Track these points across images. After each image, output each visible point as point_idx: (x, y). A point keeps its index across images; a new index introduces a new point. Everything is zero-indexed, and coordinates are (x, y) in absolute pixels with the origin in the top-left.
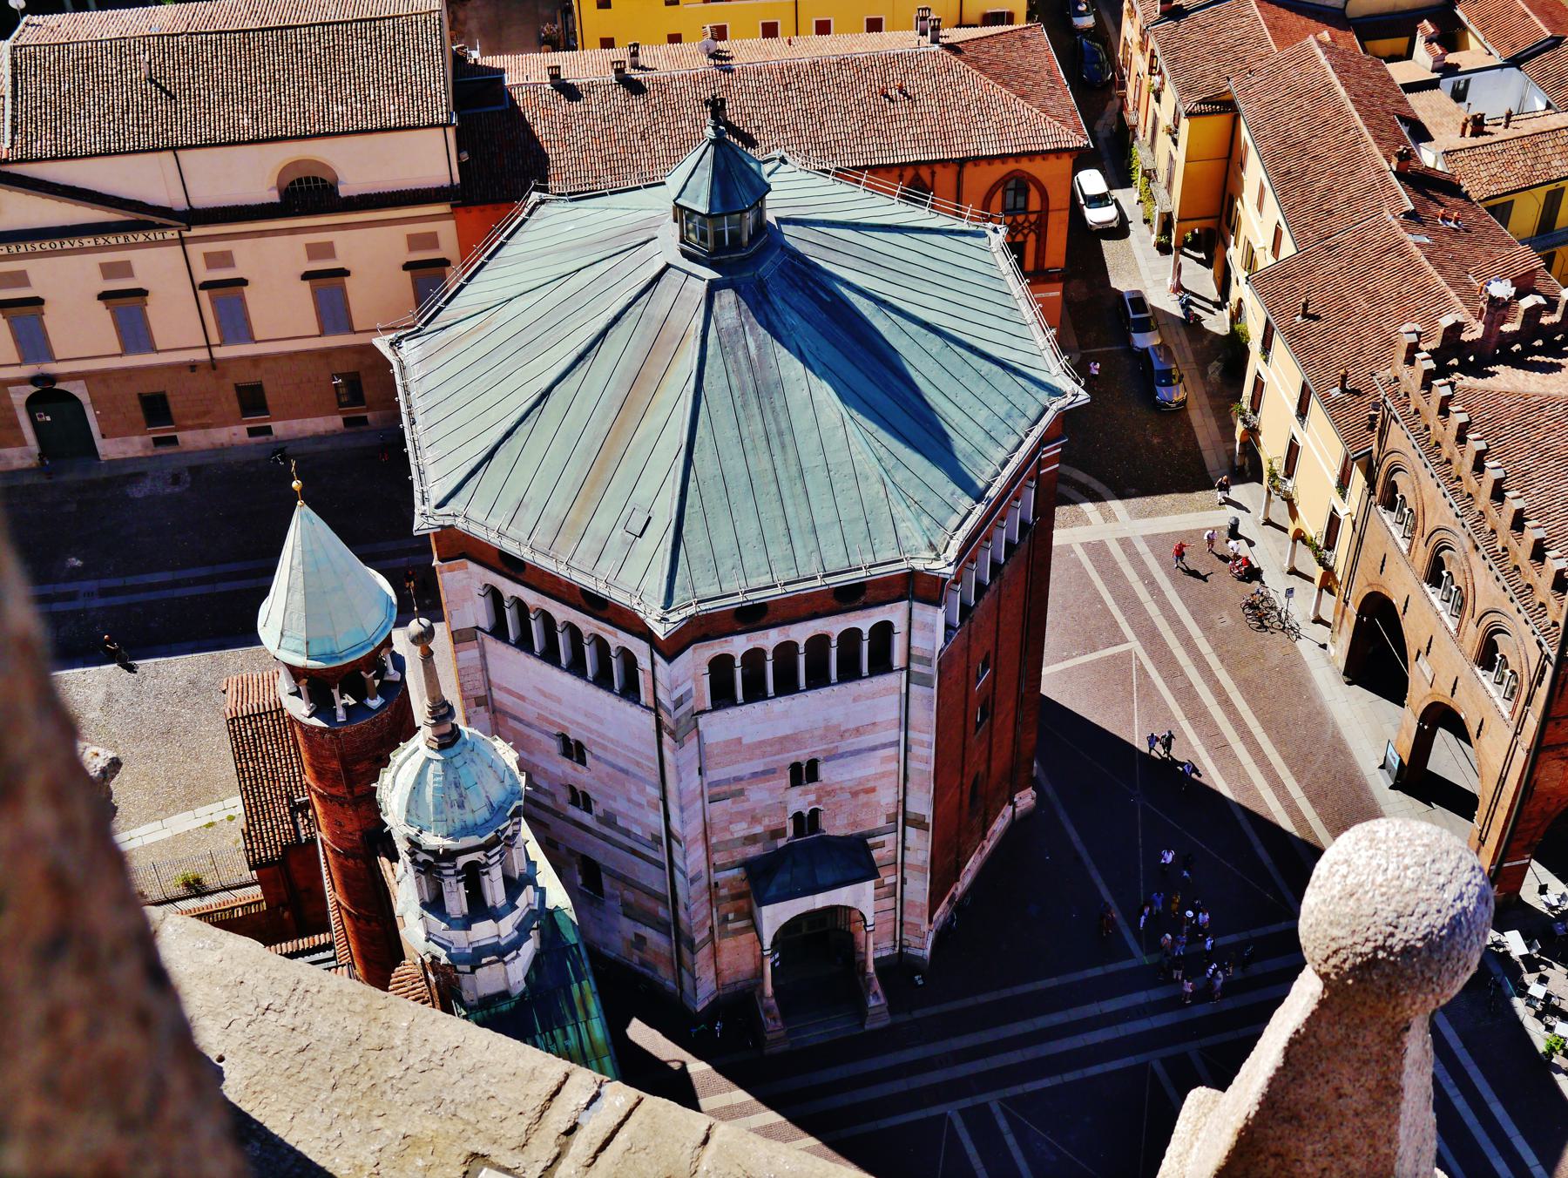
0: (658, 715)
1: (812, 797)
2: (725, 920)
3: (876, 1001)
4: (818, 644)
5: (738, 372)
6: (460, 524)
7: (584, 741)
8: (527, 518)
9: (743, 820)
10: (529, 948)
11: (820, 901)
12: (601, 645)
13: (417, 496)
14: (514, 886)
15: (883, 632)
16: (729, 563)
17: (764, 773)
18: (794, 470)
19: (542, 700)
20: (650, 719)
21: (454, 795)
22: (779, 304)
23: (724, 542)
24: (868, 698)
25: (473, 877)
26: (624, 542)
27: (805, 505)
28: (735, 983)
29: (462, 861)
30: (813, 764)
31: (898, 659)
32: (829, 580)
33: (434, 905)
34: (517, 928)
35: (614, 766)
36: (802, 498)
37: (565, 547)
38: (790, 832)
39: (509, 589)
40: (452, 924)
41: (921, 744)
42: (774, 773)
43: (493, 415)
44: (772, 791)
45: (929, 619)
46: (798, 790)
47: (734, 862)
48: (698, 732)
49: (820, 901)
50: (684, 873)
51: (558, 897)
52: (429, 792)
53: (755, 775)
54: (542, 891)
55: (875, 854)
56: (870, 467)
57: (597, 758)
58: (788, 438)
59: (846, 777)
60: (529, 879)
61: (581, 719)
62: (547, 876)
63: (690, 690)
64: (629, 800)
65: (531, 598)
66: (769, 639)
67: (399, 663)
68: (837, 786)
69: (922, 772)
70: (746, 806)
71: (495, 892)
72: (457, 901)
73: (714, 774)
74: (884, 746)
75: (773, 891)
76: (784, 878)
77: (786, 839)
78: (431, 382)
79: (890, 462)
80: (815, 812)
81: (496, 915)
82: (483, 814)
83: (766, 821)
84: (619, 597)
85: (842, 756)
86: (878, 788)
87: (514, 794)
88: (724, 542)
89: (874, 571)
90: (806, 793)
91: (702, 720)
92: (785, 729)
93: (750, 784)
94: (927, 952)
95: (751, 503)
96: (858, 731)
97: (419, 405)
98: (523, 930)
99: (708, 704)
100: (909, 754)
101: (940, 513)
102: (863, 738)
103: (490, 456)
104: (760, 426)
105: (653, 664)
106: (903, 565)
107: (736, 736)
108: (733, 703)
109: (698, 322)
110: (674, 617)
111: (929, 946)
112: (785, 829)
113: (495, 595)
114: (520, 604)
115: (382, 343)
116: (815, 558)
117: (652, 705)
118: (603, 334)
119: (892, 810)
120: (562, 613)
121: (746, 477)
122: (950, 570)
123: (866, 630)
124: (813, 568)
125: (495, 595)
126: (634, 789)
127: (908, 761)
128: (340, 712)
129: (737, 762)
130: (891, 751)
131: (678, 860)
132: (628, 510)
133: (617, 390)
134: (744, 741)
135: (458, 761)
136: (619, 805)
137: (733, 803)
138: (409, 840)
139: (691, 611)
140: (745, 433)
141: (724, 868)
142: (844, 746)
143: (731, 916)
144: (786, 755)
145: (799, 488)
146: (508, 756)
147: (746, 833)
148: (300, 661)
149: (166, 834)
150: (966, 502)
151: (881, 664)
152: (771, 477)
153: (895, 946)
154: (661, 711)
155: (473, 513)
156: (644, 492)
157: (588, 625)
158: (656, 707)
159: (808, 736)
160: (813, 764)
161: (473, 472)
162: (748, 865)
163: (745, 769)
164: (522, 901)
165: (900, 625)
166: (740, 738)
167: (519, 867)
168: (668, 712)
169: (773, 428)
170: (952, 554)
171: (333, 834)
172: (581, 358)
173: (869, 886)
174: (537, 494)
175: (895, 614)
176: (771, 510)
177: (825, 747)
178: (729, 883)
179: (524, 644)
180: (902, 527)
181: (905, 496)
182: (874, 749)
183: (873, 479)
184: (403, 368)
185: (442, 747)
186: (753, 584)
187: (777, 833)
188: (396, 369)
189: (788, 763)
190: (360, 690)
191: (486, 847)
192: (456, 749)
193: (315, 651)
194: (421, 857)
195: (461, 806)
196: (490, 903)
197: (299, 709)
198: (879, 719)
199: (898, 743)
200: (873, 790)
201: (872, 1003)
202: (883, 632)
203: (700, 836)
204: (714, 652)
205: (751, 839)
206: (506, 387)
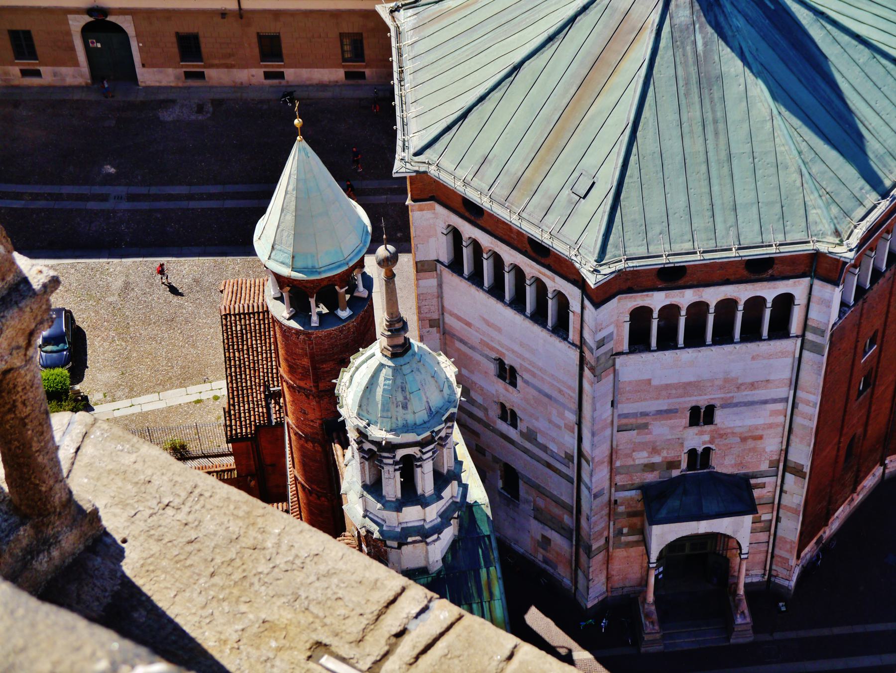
0: (582, 352)
1: (707, 438)
2: (620, 533)
3: (743, 619)
4: (727, 307)
5: (685, 64)
6: (433, 171)
7: (517, 367)
8: (490, 172)
9: (643, 450)
10: (449, 534)
11: (703, 527)
12: (541, 288)
13: (399, 143)
14: (442, 480)
15: (785, 302)
16: (657, 229)
17: (668, 412)
18: (723, 155)
19: (484, 327)
20: (574, 355)
21: (400, 398)
22: (729, 8)
23: (655, 210)
24: (764, 358)
25: (408, 467)
26: (570, 201)
27: (729, 186)
28: (623, 588)
29: (400, 453)
30: (710, 409)
31: (795, 327)
32: (743, 253)
33: (374, 488)
34: (441, 516)
35: (540, 391)
36: (728, 180)
37: (519, 199)
38: (684, 465)
39: (469, 231)
40: (386, 505)
41: (807, 403)
42: (677, 412)
43: (471, 81)
44: (672, 428)
45: (827, 296)
46: (695, 429)
47: (632, 484)
48: (615, 370)
49: (703, 527)
50: (589, 489)
51: (478, 493)
52: (379, 391)
53: (659, 412)
54: (465, 487)
55: (756, 493)
56: (790, 156)
57: (526, 382)
58: (721, 126)
59: (738, 423)
60: (455, 475)
61: (516, 348)
62: (471, 475)
63: (612, 334)
64: (550, 421)
65: (486, 241)
66: (685, 298)
67: (368, 282)
68: (729, 431)
69: (804, 427)
70: (648, 438)
71: (425, 482)
72: (392, 486)
73: (624, 408)
74: (775, 401)
75: (663, 513)
76: (674, 503)
77: (680, 470)
78: (421, 47)
79: (809, 156)
80: (707, 451)
81: (424, 502)
82: (422, 416)
83: (664, 453)
84: (559, 247)
85: (736, 405)
86: (765, 437)
87: (450, 402)
88: (655, 210)
89: (783, 249)
90: (701, 433)
91: (619, 360)
92: (689, 377)
93: (656, 419)
94: (793, 584)
95: (682, 179)
96: (753, 386)
97: (408, 66)
98: (445, 518)
99: (625, 347)
100: (796, 410)
101: (848, 204)
102: (757, 392)
103: (464, 116)
104: (698, 114)
105: (583, 308)
106: (810, 247)
107: (646, 377)
108: (647, 348)
109: (655, 17)
110: (605, 270)
111: (795, 578)
112: (680, 462)
113: (456, 235)
114: (476, 246)
115: (383, 10)
116: (733, 232)
117: (578, 343)
118: (572, 20)
119: (775, 457)
120: (510, 256)
121: (681, 156)
122: (851, 255)
124: (731, 241)
125: (456, 235)
126: (554, 412)
127: (794, 417)
128: (315, 320)
129: (645, 400)
131: (585, 477)
132: (576, 174)
133: (579, 69)
134: (655, 382)
135: (406, 369)
136: (540, 425)
137: (638, 434)
138: (359, 431)
139: (620, 266)
140: (684, 118)
141: (624, 488)
142: (741, 396)
143: (625, 530)
144: (688, 399)
145: (726, 170)
146: (449, 370)
147: (646, 461)
148: (286, 271)
149: (161, 405)
150: (872, 197)
151: (780, 330)
152: (702, 158)
153: (764, 574)
154: (585, 349)
155: (446, 163)
156: (591, 161)
157: (531, 268)
158: (581, 346)
159: (709, 384)
160: (710, 409)
161: (448, 128)
162: (645, 489)
163: (652, 406)
164: (447, 493)
165: (800, 298)
166: (649, 381)
167: (447, 464)
168: (591, 350)
169: (709, 116)
170: (854, 241)
171: (297, 419)
172: (550, 39)
173: (748, 519)
174: (500, 153)
175: (797, 288)
176: (699, 187)
177: (722, 396)
178: (627, 502)
179: (476, 278)
180: (813, 214)
181: (819, 186)
182: (765, 402)
183: (793, 169)
184: (399, 33)
185: (394, 356)
186: (677, 248)
187: (672, 464)
188: (393, 33)
189: (690, 405)
190: (333, 303)
191: (422, 444)
192: (406, 358)
193: (299, 264)
194: (367, 446)
195: (405, 407)
196: (420, 491)
197: (281, 311)
198: (772, 377)
199: (786, 400)
200: (760, 437)
201: (739, 620)
202: (785, 302)
203: (607, 459)
204: (635, 303)
206: (483, 58)
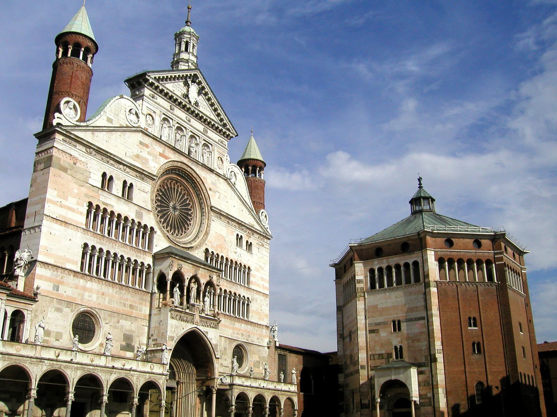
1: (399, 339)
80: (401, 347)
90: (397, 337)
100: (429, 323)
119: (426, 354)
123: (411, 263)
130: (421, 322)
134: (379, 307)
187: (389, 355)
205: (381, 356)
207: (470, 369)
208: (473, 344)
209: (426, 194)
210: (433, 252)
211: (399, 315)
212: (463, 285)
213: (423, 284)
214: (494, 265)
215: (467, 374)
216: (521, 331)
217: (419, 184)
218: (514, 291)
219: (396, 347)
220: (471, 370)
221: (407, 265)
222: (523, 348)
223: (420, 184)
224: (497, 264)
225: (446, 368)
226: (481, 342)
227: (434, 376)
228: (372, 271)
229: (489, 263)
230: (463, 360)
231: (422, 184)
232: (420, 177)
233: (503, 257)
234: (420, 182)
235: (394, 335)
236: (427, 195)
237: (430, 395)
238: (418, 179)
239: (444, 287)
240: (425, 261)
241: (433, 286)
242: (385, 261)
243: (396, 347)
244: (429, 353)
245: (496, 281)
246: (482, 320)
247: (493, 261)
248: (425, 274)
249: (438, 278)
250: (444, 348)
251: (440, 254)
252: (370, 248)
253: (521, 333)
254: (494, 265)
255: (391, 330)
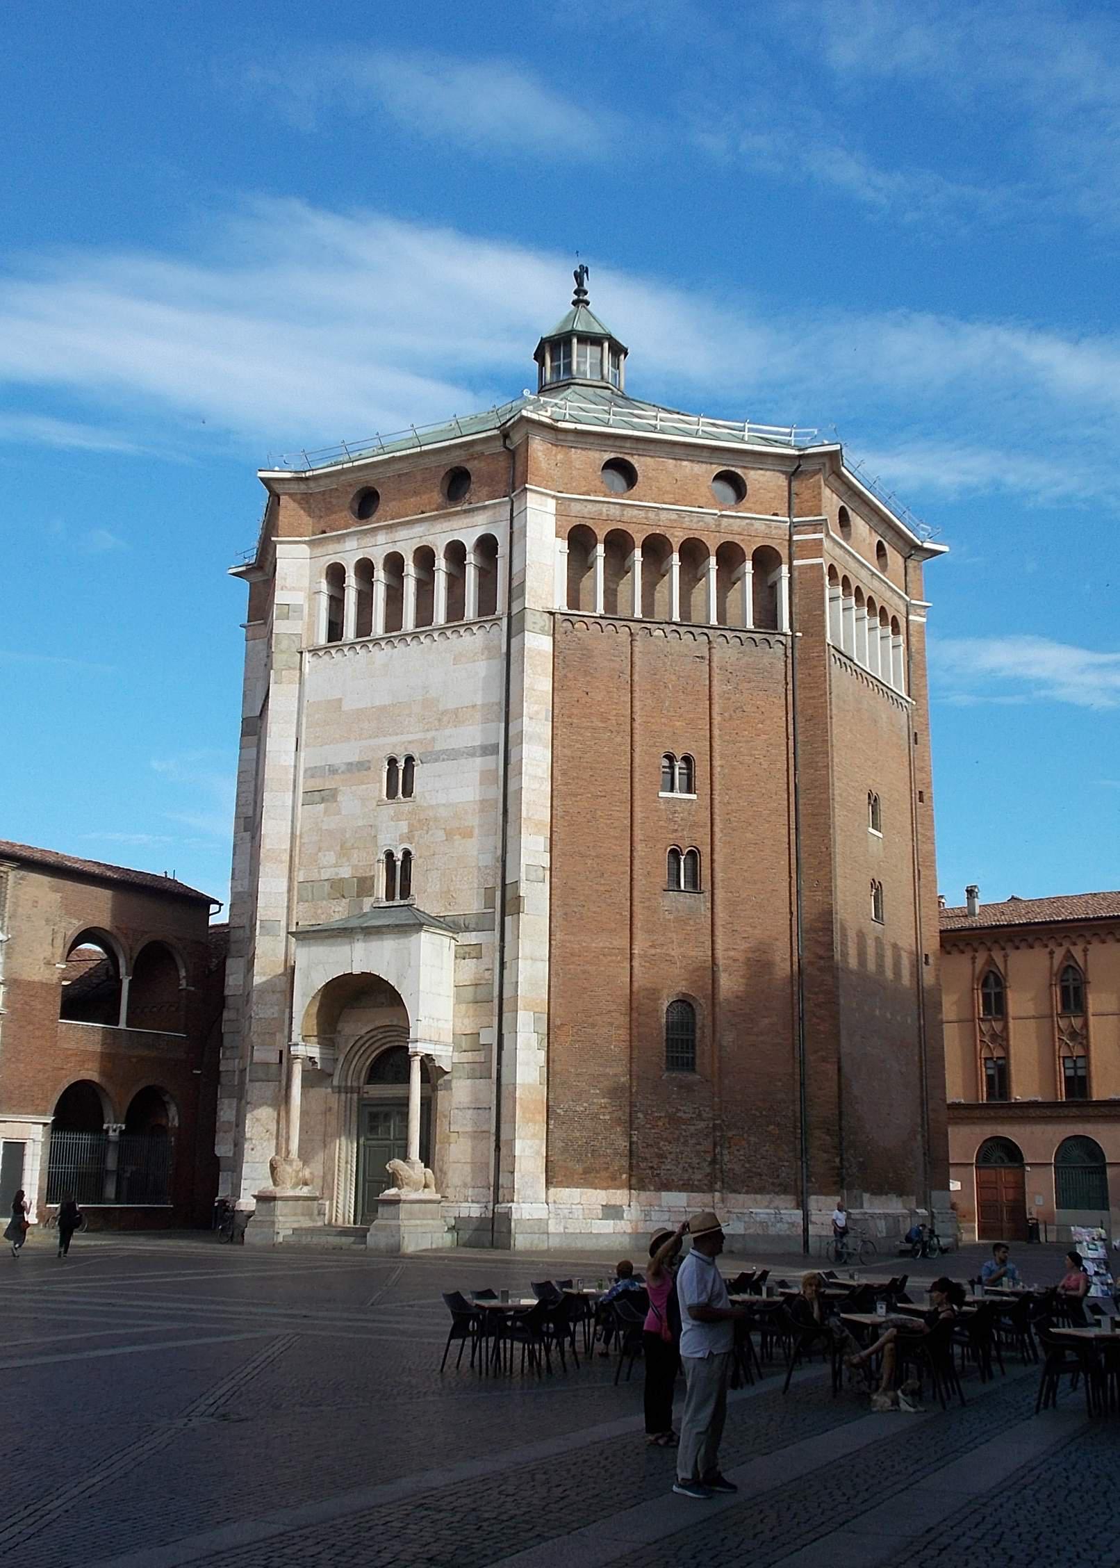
1: (404, 827)
59: (441, 798)
90: (396, 818)
123: (469, 544)
144: (381, 741)
177: (420, 736)
187: (364, 886)
205: (337, 888)
207: (653, 946)
208: (675, 854)
209: (596, 324)
210: (552, 504)
211: (411, 737)
212: (659, 633)
213: (505, 620)
214: (785, 568)
215: (635, 964)
216: (875, 826)
217: (576, 292)
218: (861, 674)
219: (390, 855)
220: (653, 951)
221: (456, 552)
222: (877, 887)
223: (580, 291)
224: (800, 567)
225: (558, 936)
226: (706, 850)
227: (508, 965)
228: (336, 574)
229: (766, 560)
230: (628, 914)
231: (586, 293)
232: (581, 267)
233: (821, 540)
234: (580, 283)
235: (390, 809)
236: (597, 329)
237: (489, 1037)
238: (575, 273)
239: (579, 635)
240: (516, 533)
241: (538, 627)
242: (381, 538)
243: (390, 855)
244: (499, 881)
245: (786, 627)
246: (717, 770)
247: (784, 553)
248: (515, 584)
249: (560, 603)
250: (557, 865)
251: (583, 512)
252: (336, 489)
253: (871, 830)
254: (785, 568)
255: (381, 791)
